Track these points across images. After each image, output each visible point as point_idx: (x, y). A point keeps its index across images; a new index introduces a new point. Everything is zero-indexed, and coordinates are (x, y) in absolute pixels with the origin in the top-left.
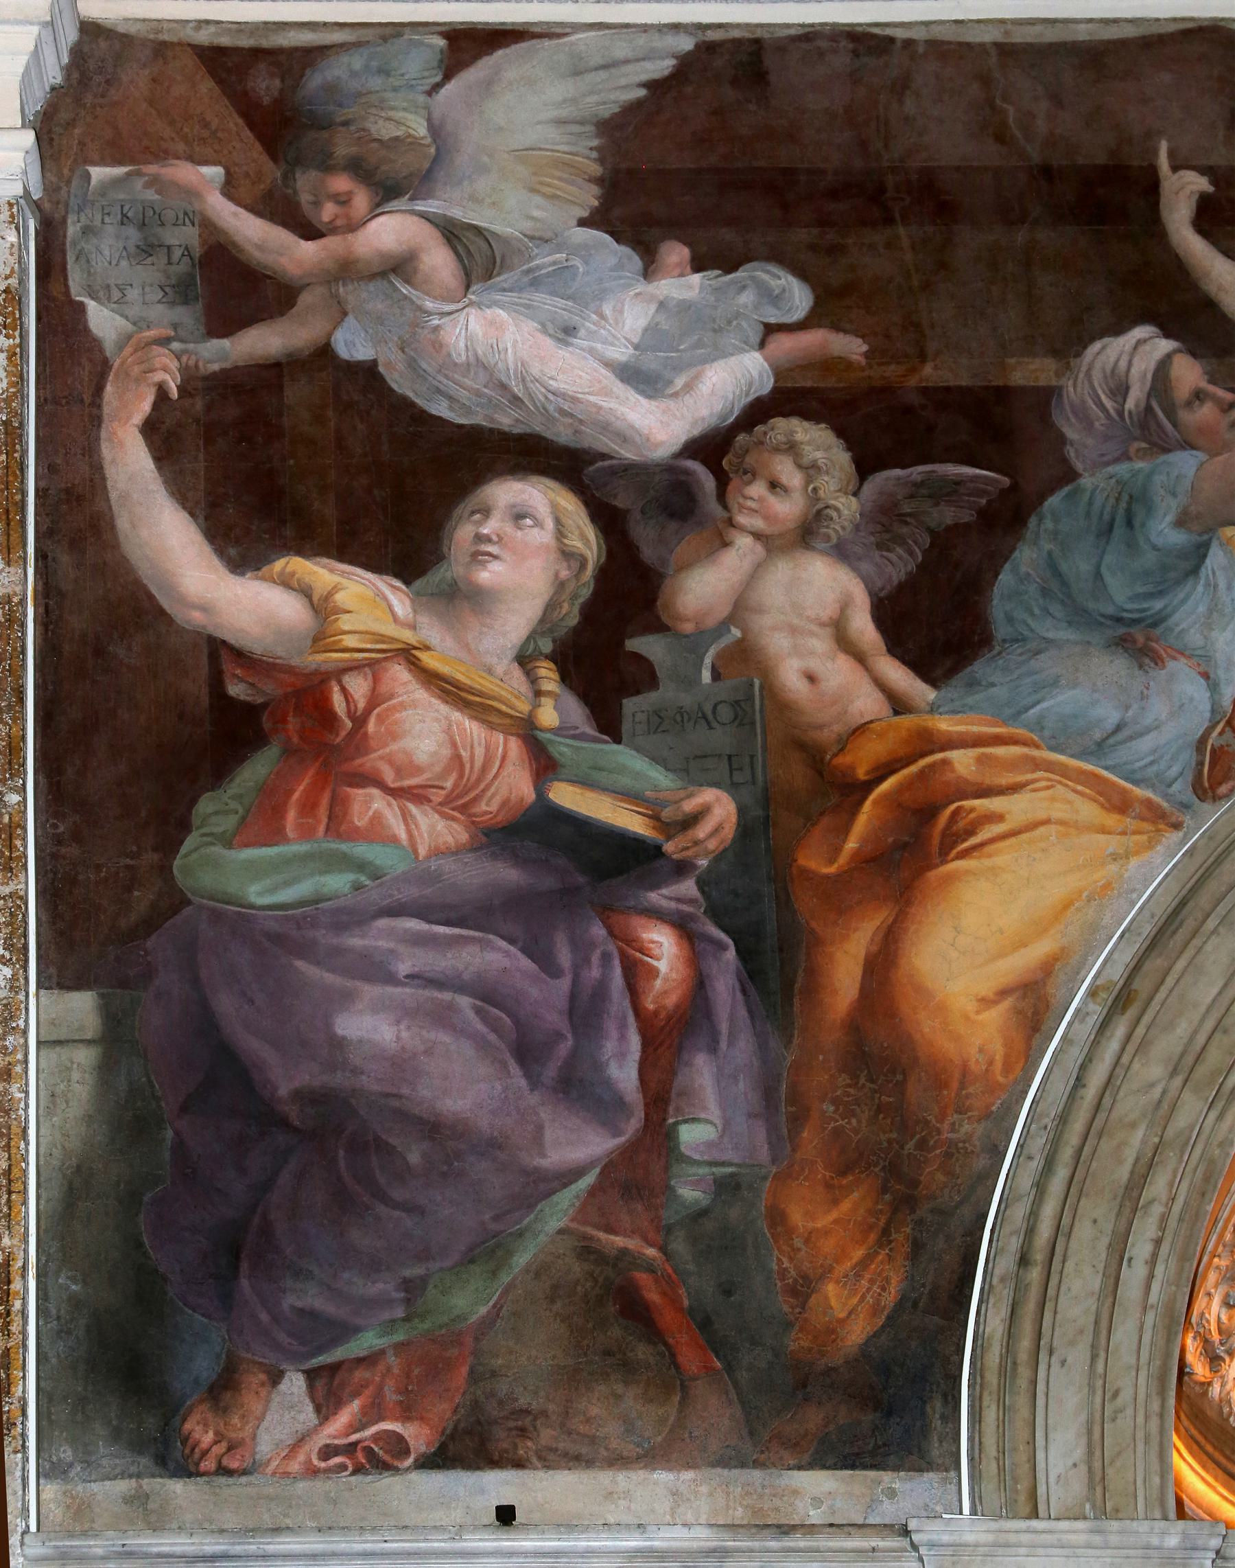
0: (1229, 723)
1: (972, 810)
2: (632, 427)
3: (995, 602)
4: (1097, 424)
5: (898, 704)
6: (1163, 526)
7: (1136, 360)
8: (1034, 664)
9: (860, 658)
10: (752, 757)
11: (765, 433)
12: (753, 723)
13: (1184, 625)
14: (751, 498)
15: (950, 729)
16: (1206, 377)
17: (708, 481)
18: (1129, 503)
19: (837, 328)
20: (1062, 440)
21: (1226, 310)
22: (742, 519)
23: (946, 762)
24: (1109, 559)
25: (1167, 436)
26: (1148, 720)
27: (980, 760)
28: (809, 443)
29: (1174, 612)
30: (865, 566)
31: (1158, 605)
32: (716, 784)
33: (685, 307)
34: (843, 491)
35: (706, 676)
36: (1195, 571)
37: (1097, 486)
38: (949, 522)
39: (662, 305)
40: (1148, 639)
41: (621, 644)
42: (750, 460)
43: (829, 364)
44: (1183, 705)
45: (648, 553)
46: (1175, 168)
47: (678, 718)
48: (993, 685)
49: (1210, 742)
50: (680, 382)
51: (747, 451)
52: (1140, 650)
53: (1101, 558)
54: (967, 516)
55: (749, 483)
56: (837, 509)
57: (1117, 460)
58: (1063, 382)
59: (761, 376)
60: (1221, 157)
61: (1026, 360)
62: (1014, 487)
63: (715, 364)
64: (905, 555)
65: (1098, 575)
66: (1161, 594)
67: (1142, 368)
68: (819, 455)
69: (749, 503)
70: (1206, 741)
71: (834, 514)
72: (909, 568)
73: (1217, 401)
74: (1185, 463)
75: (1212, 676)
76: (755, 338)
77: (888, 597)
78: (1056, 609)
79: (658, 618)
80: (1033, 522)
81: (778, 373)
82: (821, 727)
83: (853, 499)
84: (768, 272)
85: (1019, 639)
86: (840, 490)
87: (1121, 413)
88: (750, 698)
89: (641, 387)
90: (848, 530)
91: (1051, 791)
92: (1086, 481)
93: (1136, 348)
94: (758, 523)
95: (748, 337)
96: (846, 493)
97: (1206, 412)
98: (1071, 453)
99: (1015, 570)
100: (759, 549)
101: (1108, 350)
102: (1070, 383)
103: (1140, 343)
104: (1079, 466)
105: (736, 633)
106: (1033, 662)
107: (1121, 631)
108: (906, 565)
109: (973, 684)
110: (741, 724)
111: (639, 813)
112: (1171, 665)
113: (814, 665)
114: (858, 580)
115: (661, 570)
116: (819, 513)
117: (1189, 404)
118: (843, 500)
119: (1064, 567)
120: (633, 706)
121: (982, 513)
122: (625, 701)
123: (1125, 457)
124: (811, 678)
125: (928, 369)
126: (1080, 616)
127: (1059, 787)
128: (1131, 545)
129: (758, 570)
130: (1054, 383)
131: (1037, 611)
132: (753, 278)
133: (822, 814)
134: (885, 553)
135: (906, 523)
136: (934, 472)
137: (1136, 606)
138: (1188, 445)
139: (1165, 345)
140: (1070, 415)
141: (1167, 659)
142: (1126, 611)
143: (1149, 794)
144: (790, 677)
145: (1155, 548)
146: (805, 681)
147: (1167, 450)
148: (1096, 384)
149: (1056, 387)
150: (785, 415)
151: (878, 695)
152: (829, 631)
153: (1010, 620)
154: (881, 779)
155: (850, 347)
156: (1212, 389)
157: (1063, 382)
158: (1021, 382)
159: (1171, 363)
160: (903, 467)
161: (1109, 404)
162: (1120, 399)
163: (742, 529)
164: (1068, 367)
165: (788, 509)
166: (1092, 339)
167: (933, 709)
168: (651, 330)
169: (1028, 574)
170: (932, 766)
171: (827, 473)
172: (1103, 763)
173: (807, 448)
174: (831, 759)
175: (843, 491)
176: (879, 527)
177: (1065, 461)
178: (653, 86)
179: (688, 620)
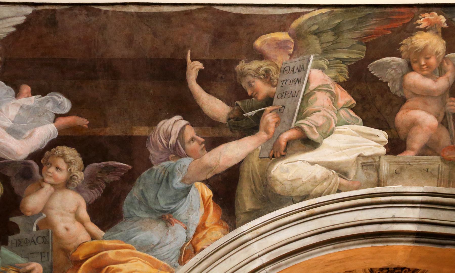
0: (191, 242)
1: (113, 268)
2: (12, 149)
3: (124, 206)
4: (160, 149)
5: (93, 237)
6: (177, 182)
7: (174, 127)
8: (135, 225)
9: (82, 223)
10: (48, 253)
11: (55, 151)
12: (49, 243)
13: (180, 213)
14: (50, 173)
15: (108, 244)
16: (196, 133)
17: (36, 167)
18: (168, 175)
19: (79, 116)
20: (149, 153)
21: (204, 110)
22: (47, 179)
23: (106, 254)
24: (160, 192)
25: (181, 152)
26: (167, 241)
27: (117, 254)
28: (69, 154)
29: (178, 209)
30: (86, 195)
31: (173, 206)
32: (37, 261)
33: (29, 108)
34: (79, 170)
35: (35, 229)
36: (186, 196)
37: (158, 169)
38: (112, 180)
39: (21, 107)
40: (170, 217)
41: (8, 219)
42: (50, 160)
43: (75, 128)
44: (178, 237)
45: (17, 190)
46: (192, 60)
47: (26, 242)
48: (122, 231)
49: (185, 248)
50: (27, 134)
51: (49, 157)
52: (167, 220)
53: (158, 192)
54: (117, 178)
55: (50, 167)
56: (77, 176)
57: (165, 160)
58: (150, 134)
59: (54, 132)
60: (208, 57)
61: (139, 127)
62: (132, 169)
63: (39, 128)
64: (97, 191)
65: (156, 197)
66: (175, 203)
67: (176, 129)
68: (72, 158)
69: (49, 174)
70: (184, 248)
71: (76, 178)
72: (99, 195)
73: (198, 141)
74: (186, 161)
75: (188, 228)
76: (52, 119)
77: (92, 204)
78: (143, 208)
79: (20, 211)
80: (138, 179)
81: (59, 131)
82: (69, 244)
83: (82, 173)
84: (56, 96)
85: (130, 217)
86: (78, 170)
87: (168, 145)
88: (48, 235)
89: (14, 135)
90: (80, 183)
91: (136, 263)
92: (155, 167)
93: (174, 123)
94: (52, 181)
95: (50, 119)
96: (80, 171)
97: (194, 145)
98: (151, 157)
99: (131, 195)
100: (52, 189)
101: (165, 124)
102: (153, 135)
103: (176, 121)
104: (153, 162)
105: (44, 215)
106: (134, 224)
107: (162, 214)
108: (98, 194)
109: (117, 231)
110: (45, 243)
111: (13, 270)
112: (176, 225)
113: (68, 225)
114: (83, 198)
115: (21, 196)
116: (71, 177)
117: (189, 142)
118: (79, 173)
119: (146, 195)
120: (11, 238)
121: (122, 177)
122: (9, 237)
123: (168, 159)
124: (67, 229)
125: (108, 129)
126: (150, 210)
127: (139, 261)
128: (168, 187)
129: (51, 196)
130: (147, 135)
131: (137, 208)
132: (52, 98)
133: (68, 270)
134: (92, 190)
135: (99, 181)
136: (108, 164)
137: (167, 207)
138: (187, 156)
139: (184, 122)
140: (152, 146)
141: (174, 223)
142: (164, 208)
143: (165, 263)
144: (60, 228)
145: (174, 188)
146: (65, 230)
147: (181, 157)
148: (161, 135)
149: (148, 136)
150: (62, 145)
151: (88, 234)
152: (72, 215)
153: (128, 211)
154: (86, 259)
155: (83, 122)
156: (197, 137)
157: (150, 134)
158: (138, 134)
159: (185, 128)
160: (99, 162)
161: (164, 142)
162: (168, 140)
163: (47, 182)
164: (152, 129)
165: (62, 176)
166: (161, 120)
167: (104, 238)
168: (18, 116)
169: (135, 197)
170: (102, 255)
171: (74, 164)
172: (154, 254)
173: (68, 156)
174: (72, 254)
175: (79, 170)
176: (90, 182)
177: (149, 160)
178: (17, 26)
179: (29, 212)
